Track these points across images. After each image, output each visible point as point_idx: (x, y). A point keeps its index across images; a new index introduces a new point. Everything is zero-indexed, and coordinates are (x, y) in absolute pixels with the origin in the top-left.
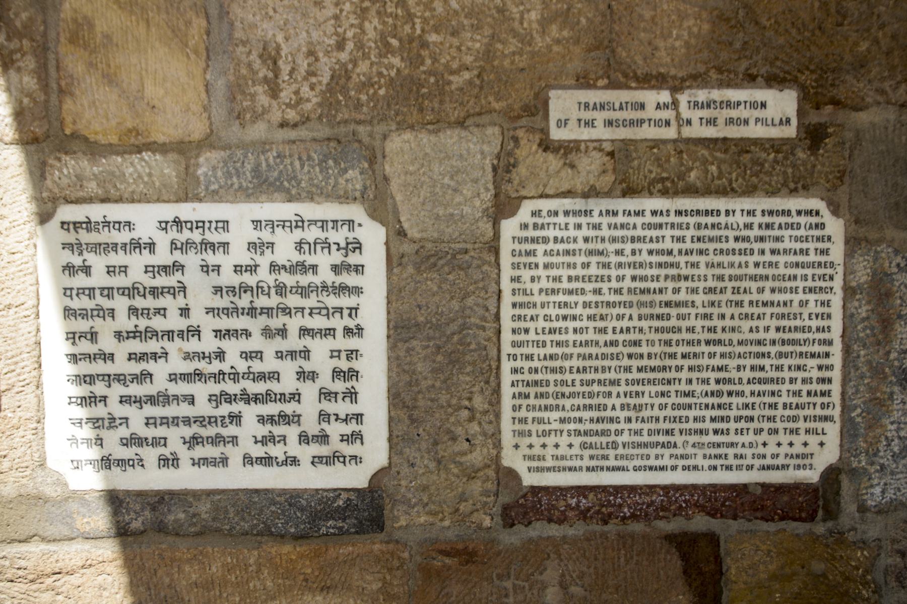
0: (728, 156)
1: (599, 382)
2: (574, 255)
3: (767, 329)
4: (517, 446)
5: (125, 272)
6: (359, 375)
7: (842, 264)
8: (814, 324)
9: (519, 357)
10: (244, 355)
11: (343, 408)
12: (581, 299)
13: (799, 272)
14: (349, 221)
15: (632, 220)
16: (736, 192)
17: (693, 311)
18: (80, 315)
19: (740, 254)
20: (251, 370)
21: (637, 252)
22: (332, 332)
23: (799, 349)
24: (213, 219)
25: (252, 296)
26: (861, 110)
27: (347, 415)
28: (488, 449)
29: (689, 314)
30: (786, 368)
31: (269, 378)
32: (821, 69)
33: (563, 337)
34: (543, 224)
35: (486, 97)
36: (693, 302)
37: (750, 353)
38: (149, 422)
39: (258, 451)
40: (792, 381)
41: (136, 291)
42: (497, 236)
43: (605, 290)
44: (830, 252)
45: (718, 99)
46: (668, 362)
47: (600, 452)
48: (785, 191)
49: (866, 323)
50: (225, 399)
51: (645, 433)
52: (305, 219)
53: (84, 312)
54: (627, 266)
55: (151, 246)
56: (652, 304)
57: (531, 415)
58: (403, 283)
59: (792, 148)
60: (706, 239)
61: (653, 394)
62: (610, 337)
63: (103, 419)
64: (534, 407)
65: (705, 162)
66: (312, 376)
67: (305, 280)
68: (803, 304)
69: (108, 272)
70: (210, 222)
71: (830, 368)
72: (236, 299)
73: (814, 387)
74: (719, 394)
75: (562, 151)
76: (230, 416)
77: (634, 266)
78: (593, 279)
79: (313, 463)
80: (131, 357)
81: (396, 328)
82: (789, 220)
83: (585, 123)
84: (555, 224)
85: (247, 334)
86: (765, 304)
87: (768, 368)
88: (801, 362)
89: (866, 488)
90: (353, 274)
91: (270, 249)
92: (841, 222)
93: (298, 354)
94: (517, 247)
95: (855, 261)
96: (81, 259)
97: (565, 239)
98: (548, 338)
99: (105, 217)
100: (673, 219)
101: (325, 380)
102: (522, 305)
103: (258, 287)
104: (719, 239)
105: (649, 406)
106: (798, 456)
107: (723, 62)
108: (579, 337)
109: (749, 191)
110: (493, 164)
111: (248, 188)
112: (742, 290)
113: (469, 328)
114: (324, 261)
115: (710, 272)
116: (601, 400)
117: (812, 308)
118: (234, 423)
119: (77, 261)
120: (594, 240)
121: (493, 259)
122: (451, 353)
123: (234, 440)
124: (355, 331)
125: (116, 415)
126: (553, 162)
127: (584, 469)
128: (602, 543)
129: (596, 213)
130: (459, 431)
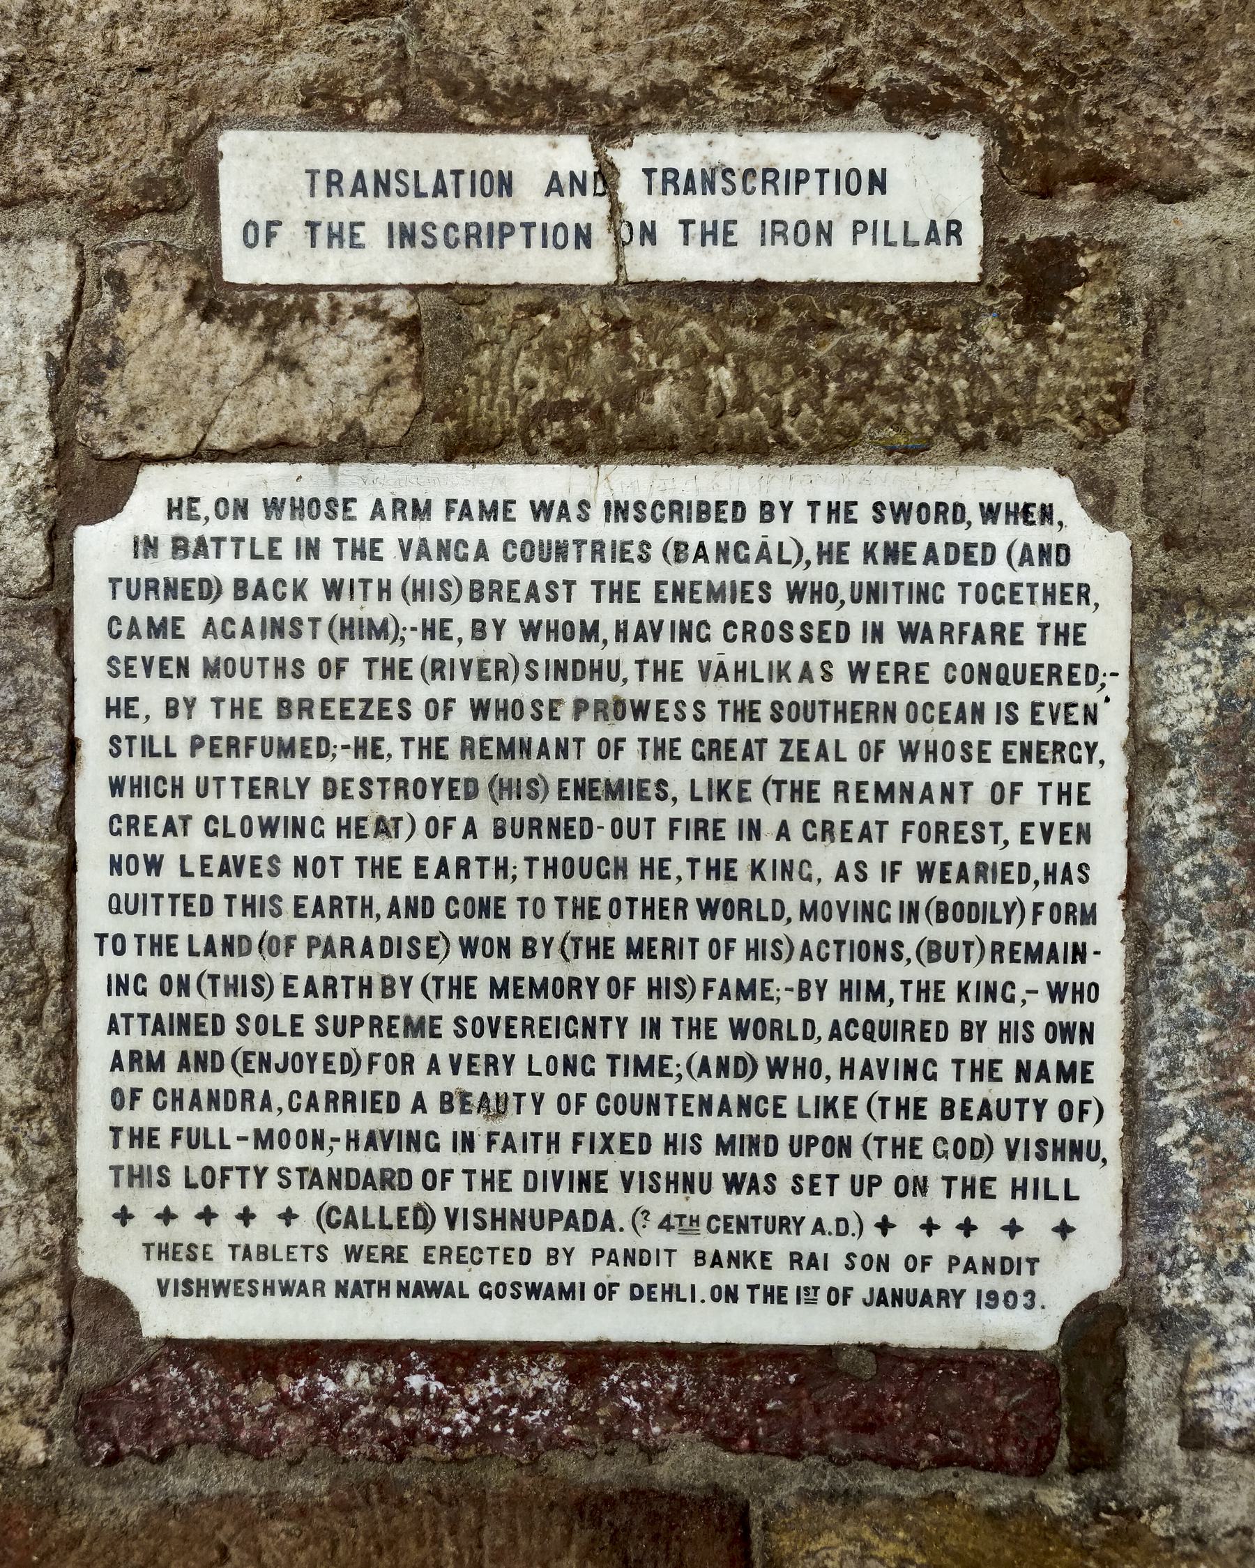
0: (769, 339)
1: (375, 1023)
2: (297, 634)
3: (891, 871)
4: (124, 1216)
7: (1124, 672)
8: (1038, 855)
9: (132, 945)
12: (317, 770)
13: (991, 695)
15: (472, 531)
16: (794, 447)
17: (662, 812)
19: (807, 639)
21: (491, 630)
23: (990, 933)
26: (1183, 196)
28: (37, 1223)
29: (650, 820)
30: (950, 992)
32: (1060, 71)
33: (262, 887)
34: (201, 542)
35: (29, 152)
36: (661, 783)
37: (839, 943)
40: (969, 1031)
42: (60, 574)
43: (392, 745)
44: (1087, 634)
45: (738, 163)
46: (586, 967)
47: (378, 1237)
48: (946, 444)
49: (1199, 858)
51: (515, 1181)
54: (459, 672)
56: (535, 789)
57: (167, 1120)
59: (966, 314)
60: (702, 592)
61: (539, 1066)
62: (406, 886)
64: (178, 1098)
65: (699, 357)
68: (1002, 794)
71: (1087, 992)
73: (1040, 1051)
74: (744, 1067)
75: (259, 319)
77: (482, 670)
78: (356, 709)
82: (959, 534)
83: (331, 236)
84: (238, 541)
86: (884, 794)
87: (894, 990)
88: (998, 973)
89: (1208, 1375)
92: (1119, 542)
94: (125, 608)
95: (1164, 663)
97: (269, 586)
98: (218, 887)
100: (599, 528)
102: (140, 787)
104: (741, 592)
105: (527, 1102)
106: (988, 1266)
107: (751, 48)
108: (311, 887)
109: (834, 445)
110: (49, 357)
112: (812, 750)
115: (713, 693)
116: (380, 1081)
117: (1030, 806)
120: (359, 590)
121: (48, 645)
126: (235, 350)
127: (330, 1289)
128: (387, 1520)
129: (362, 509)
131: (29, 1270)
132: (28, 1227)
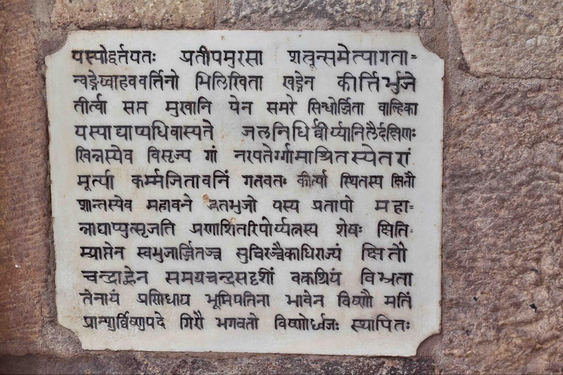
5: (145, 109)
6: (409, 229)
10: (277, 205)
11: (390, 266)
14: (401, 52)
18: (94, 156)
20: (286, 221)
22: (378, 179)
24: (245, 48)
25: (288, 138)
27: (394, 274)
28: (557, 317)
31: (306, 231)
38: (170, 277)
39: (291, 312)
41: (156, 131)
50: (256, 253)
52: (350, 49)
53: (99, 153)
55: (174, 80)
58: (463, 125)
63: (120, 273)
66: (356, 229)
67: (348, 120)
69: (125, 109)
70: (241, 52)
72: (269, 141)
76: (260, 273)
79: (353, 327)
80: (151, 204)
81: (453, 177)
85: (281, 180)
90: (405, 113)
91: (309, 84)
93: (339, 205)
96: (95, 93)
99: (121, 45)
101: (369, 234)
103: (294, 128)
111: (285, 13)
113: (539, 179)
114: (371, 98)
118: (265, 280)
119: (90, 95)
122: (518, 206)
123: (265, 299)
124: (405, 179)
125: (134, 269)
130: (524, 297)
131: (553, 335)
132: (553, 319)
